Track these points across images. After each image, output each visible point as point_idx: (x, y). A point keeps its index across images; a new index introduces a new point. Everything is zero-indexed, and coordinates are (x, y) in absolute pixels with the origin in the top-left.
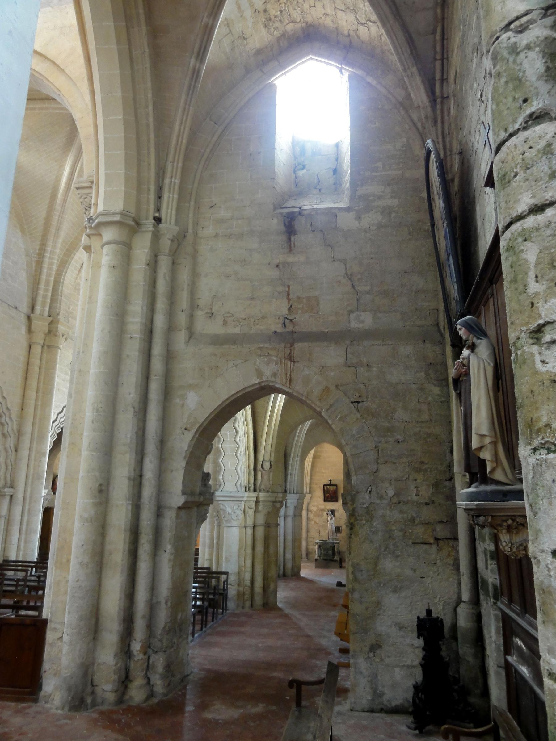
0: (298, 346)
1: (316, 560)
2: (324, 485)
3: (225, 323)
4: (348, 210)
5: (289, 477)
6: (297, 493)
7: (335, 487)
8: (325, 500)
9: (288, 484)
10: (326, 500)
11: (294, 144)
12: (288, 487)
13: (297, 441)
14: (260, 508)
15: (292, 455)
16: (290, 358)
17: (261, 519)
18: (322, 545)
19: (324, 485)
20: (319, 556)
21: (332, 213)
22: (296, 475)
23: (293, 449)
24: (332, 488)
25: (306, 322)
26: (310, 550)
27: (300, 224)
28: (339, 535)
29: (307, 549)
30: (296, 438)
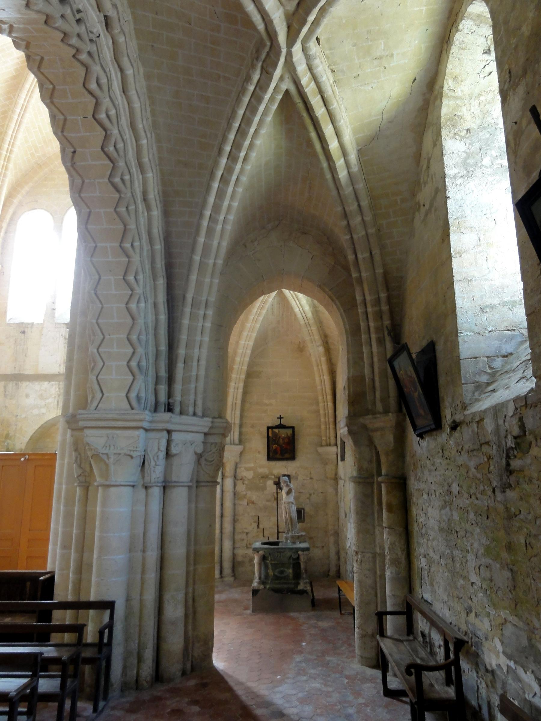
2: (268, 428)
5: (180, 365)
6: (204, 416)
7: (290, 432)
8: (270, 458)
9: (178, 387)
12: (177, 397)
13: (206, 248)
15: (189, 296)
20: (262, 582)
22: (203, 362)
23: (194, 277)
24: (283, 433)
26: (239, 559)
29: (234, 556)
30: (201, 240)
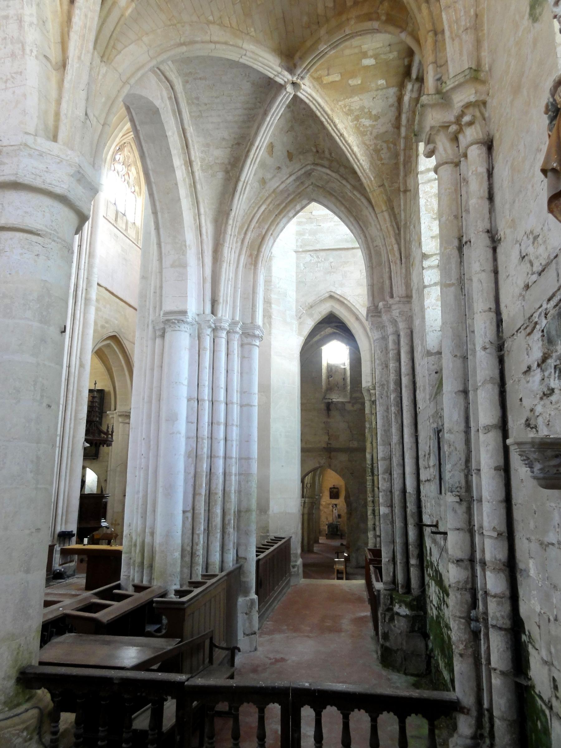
0: (332, 453)
1: (326, 534)
3: (306, 443)
4: (349, 402)
7: (337, 490)
8: (331, 498)
10: (331, 497)
11: (328, 364)
14: (306, 505)
16: (330, 458)
17: (306, 511)
18: (330, 526)
19: (330, 488)
20: (329, 532)
21: (343, 403)
24: (335, 490)
25: (335, 444)
27: (332, 407)
28: (339, 520)
